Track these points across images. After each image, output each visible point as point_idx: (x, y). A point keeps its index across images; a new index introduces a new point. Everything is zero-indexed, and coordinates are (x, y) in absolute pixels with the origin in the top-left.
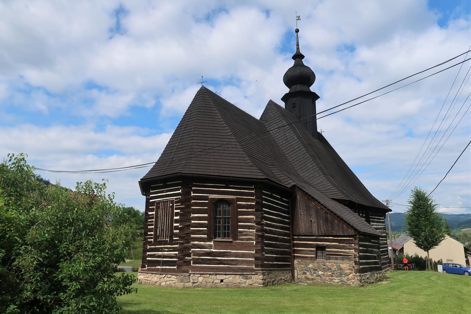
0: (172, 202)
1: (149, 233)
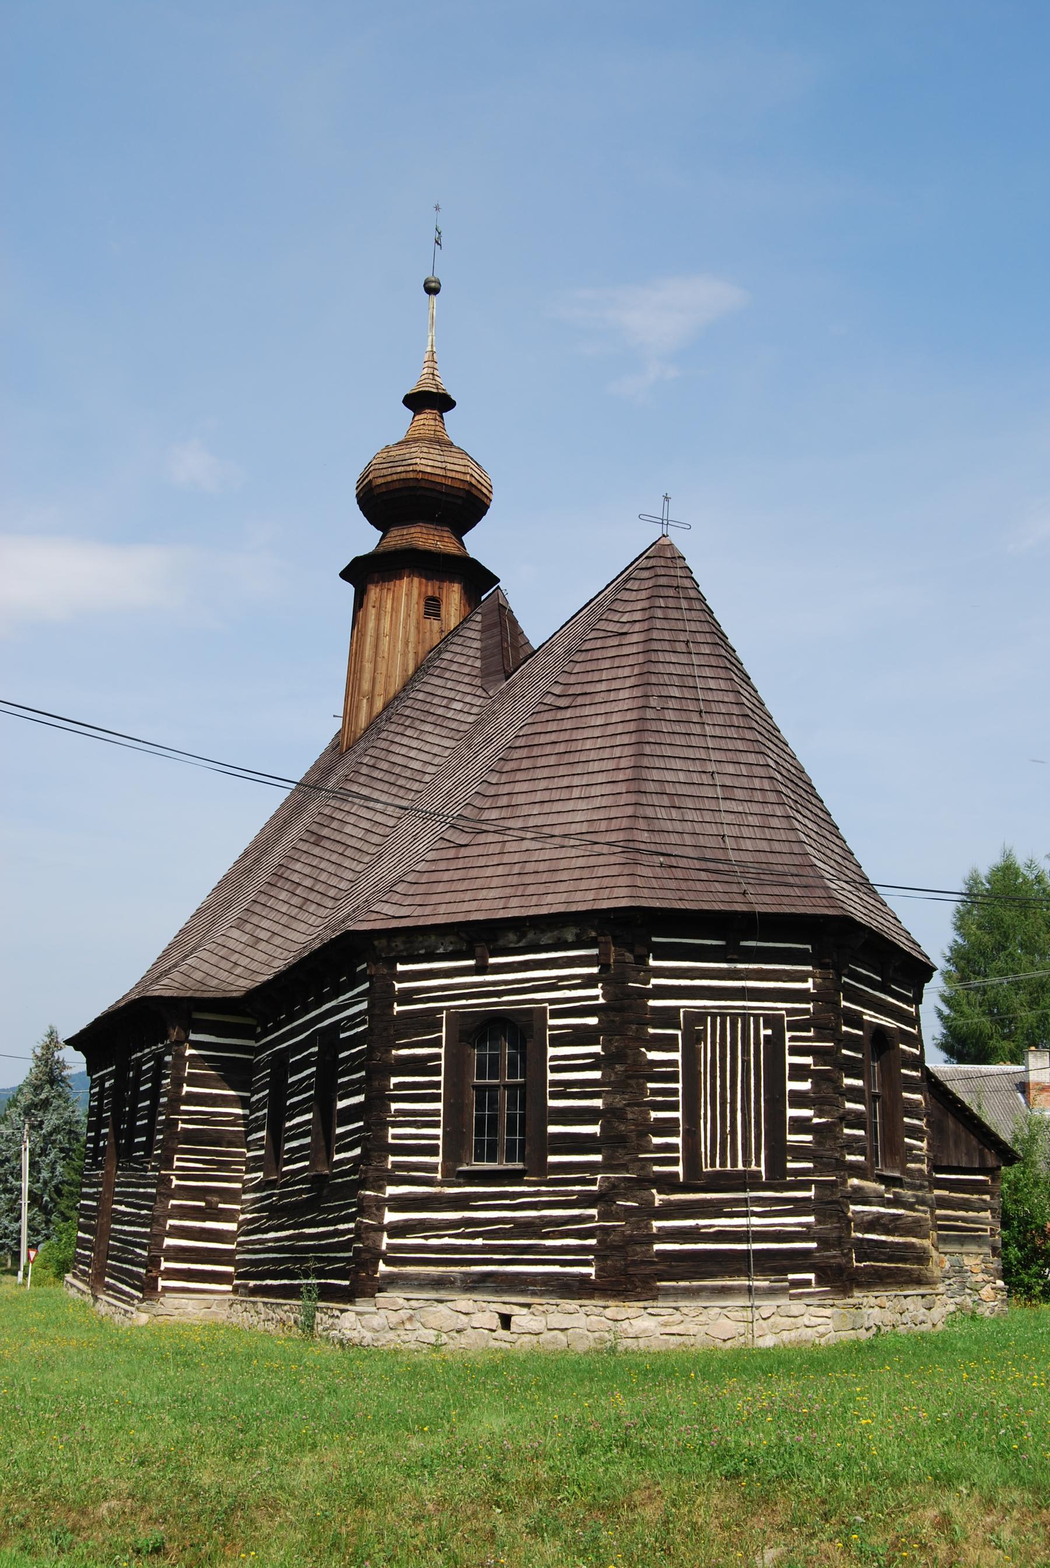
0: (773, 1021)
1: (656, 1140)
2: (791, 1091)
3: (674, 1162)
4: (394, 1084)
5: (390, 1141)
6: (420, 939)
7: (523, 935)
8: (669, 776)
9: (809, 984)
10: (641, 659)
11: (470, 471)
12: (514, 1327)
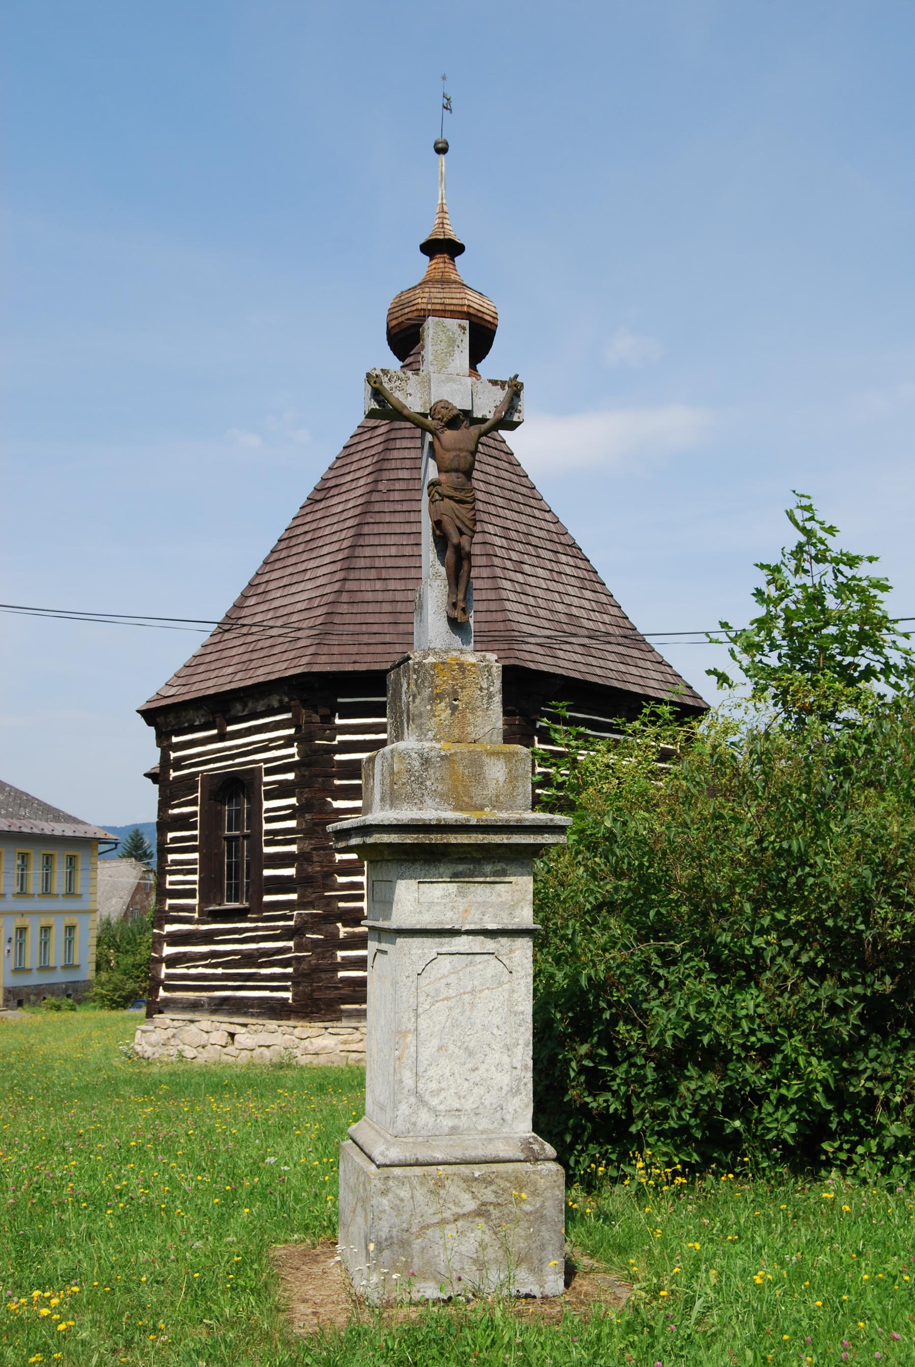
1: (341, 880)
3: (360, 898)
5: (168, 887)
6: (184, 714)
7: (245, 706)
8: (381, 551)
10: (381, 448)
11: (467, 302)
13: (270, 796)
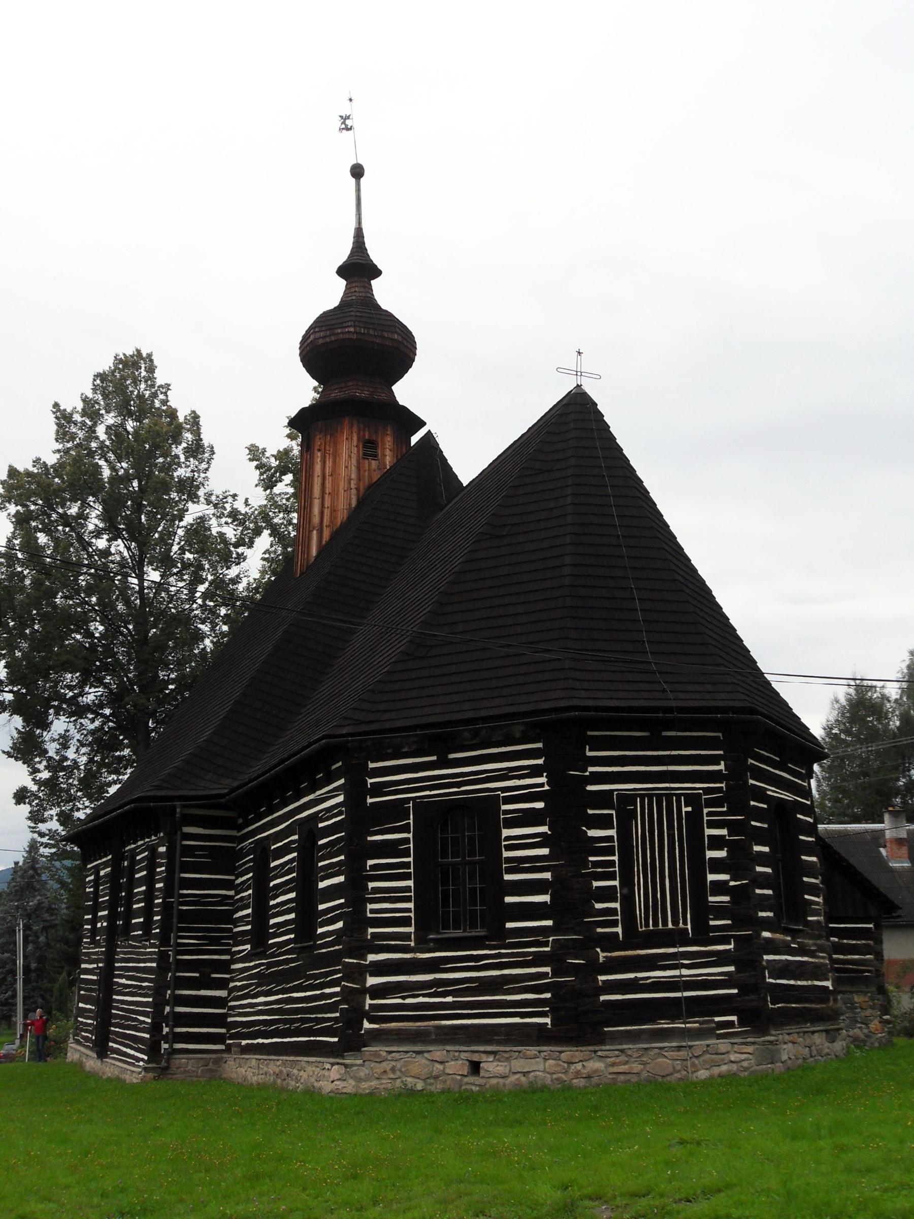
0: (692, 800)
1: (599, 906)
2: (710, 859)
3: (614, 924)
4: (370, 866)
5: (369, 915)
9: (721, 767)
12: (482, 1073)
13: (512, 823)
